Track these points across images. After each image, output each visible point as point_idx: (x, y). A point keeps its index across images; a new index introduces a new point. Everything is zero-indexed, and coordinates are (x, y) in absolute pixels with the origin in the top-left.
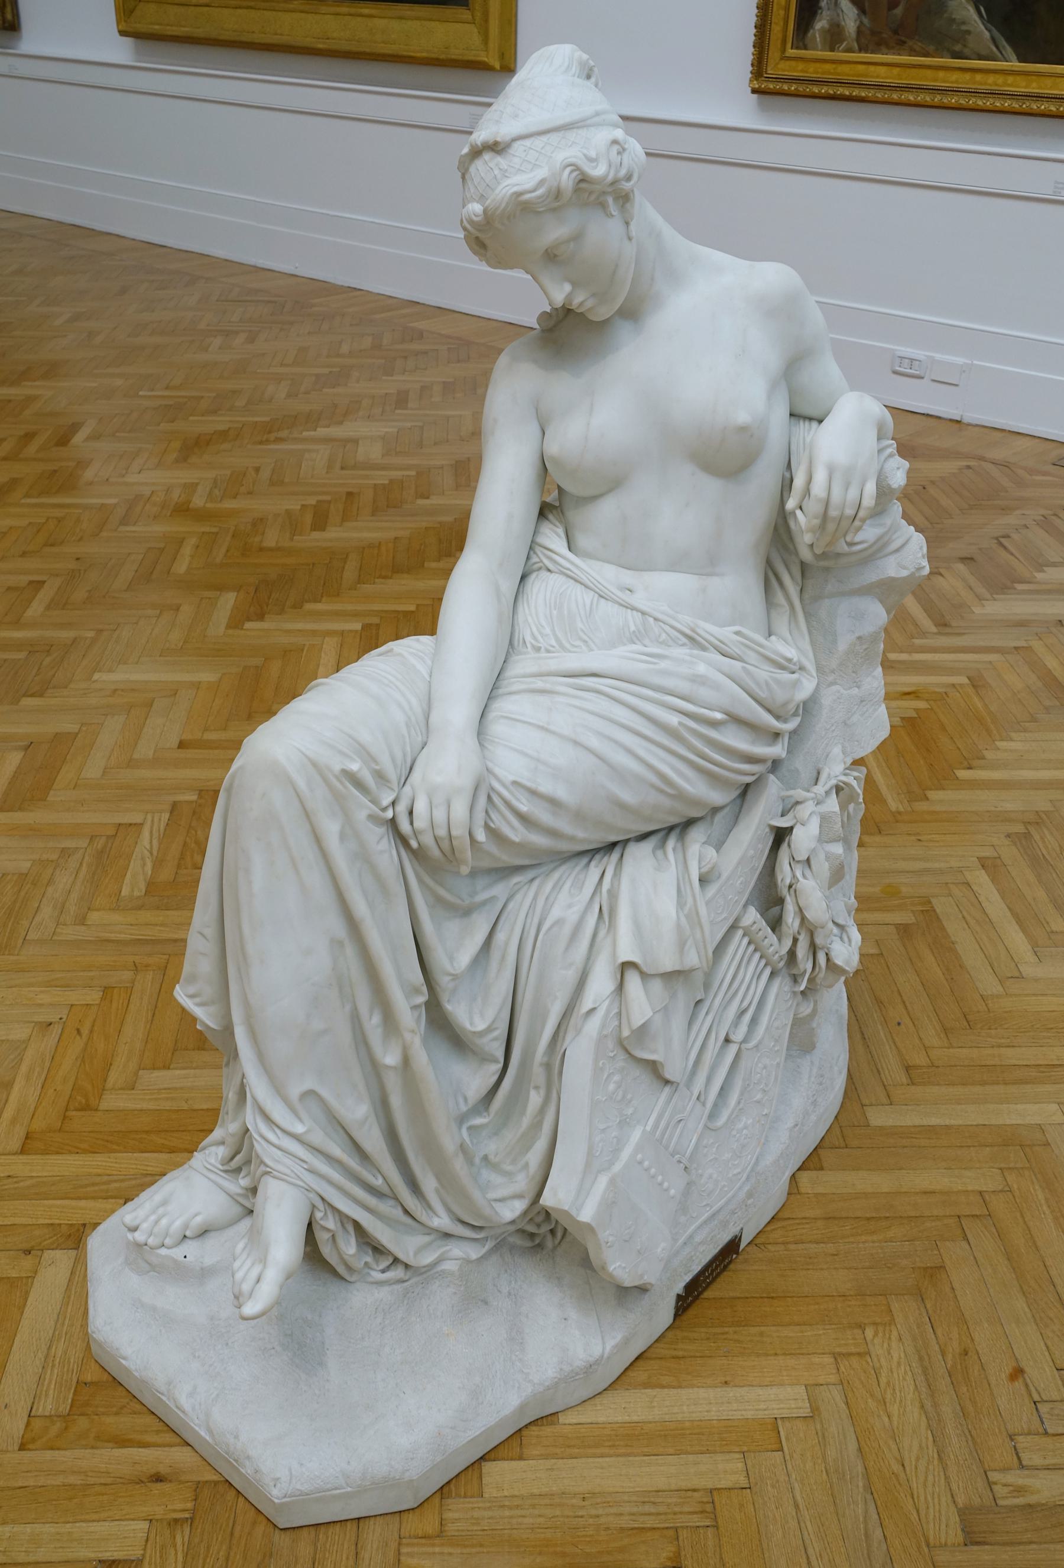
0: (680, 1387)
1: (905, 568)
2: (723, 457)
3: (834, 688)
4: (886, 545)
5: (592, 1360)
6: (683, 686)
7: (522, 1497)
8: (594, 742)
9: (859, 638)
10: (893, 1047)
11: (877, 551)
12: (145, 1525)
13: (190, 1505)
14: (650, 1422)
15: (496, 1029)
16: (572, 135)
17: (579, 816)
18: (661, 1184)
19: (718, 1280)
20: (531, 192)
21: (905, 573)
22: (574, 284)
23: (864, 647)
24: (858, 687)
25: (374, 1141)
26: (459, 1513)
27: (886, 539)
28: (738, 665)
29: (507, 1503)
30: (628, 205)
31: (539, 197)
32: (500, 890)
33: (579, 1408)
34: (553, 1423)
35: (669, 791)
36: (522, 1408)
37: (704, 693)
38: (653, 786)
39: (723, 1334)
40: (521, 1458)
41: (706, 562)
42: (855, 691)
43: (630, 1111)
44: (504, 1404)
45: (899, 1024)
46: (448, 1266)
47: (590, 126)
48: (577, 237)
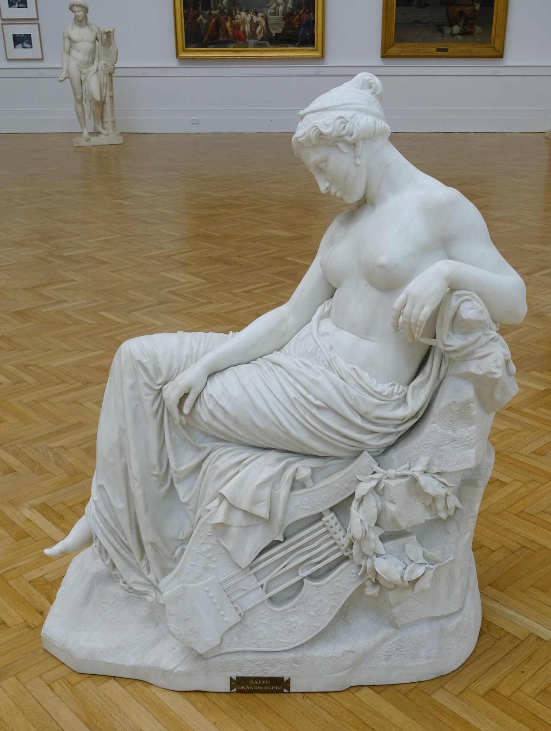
0: (200, 711)
1: (482, 370)
2: (387, 282)
3: (434, 425)
4: (472, 353)
5: (166, 669)
6: (306, 382)
7: (106, 696)
8: (251, 391)
9: (454, 402)
10: (501, 678)
11: (466, 354)
12: (22, 621)
13: (37, 625)
14: (173, 712)
15: (190, 505)
16: (324, 113)
17: (236, 421)
18: (219, 610)
19: (270, 695)
20: (302, 137)
21: (480, 372)
22: (331, 184)
23: (458, 409)
24: (454, 432)
25: (124, 520)
26: (88, 686)
27: (470, 349)
28: (342, 382)
29: (100, 694)
30: (356, 149)
31: (304, 140)
32: (209, 446)
33: (161, 690)
34: (147, 686)
35: (283, 429)
36: (134, 668)
37: (315, 389)
38: (273, 422)
39: (241, 710)
40: (123, 687)
41: (365, 332)
42: (451, 432)
43: (213, 566)
44: (128, 660)
45: (523, 672)
46: (149, 598)
47: (337, 110)
48: (326, 161)
